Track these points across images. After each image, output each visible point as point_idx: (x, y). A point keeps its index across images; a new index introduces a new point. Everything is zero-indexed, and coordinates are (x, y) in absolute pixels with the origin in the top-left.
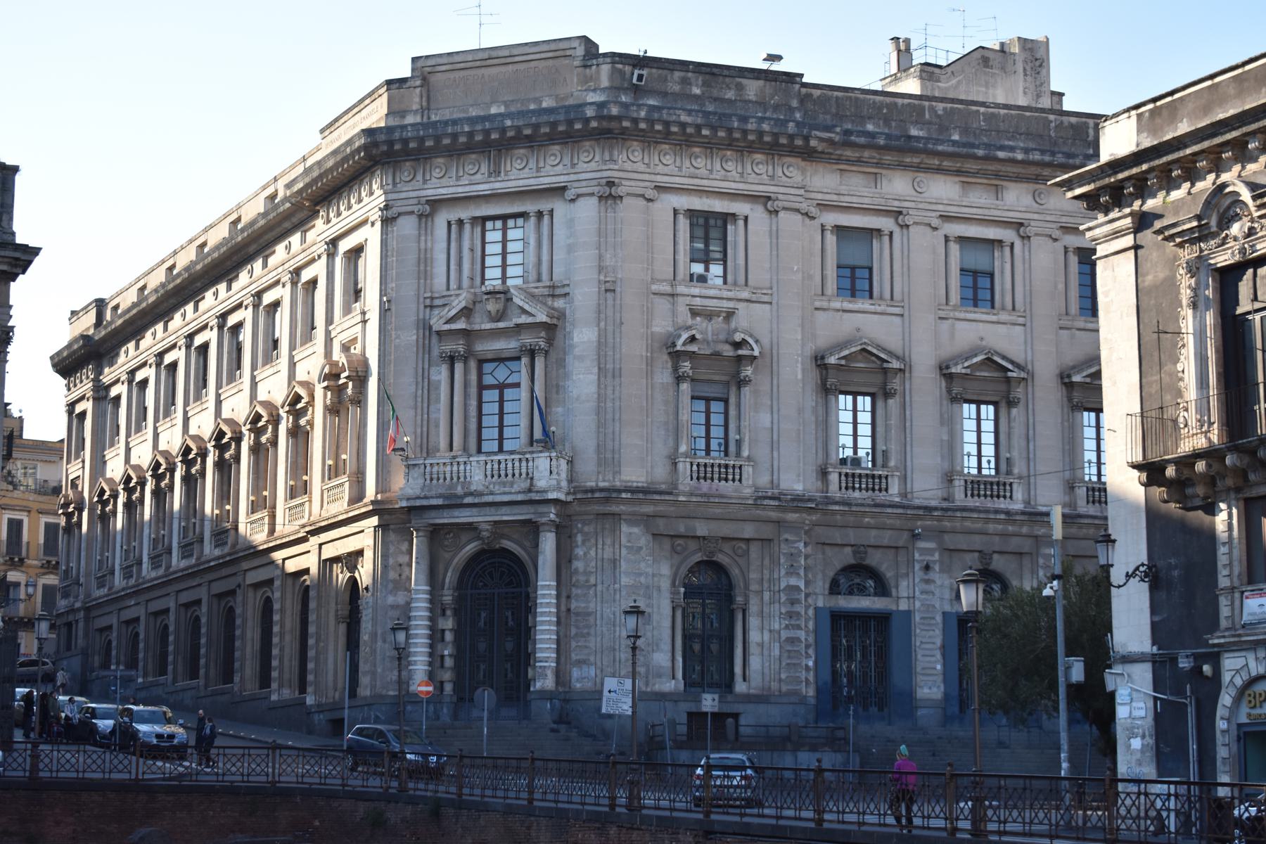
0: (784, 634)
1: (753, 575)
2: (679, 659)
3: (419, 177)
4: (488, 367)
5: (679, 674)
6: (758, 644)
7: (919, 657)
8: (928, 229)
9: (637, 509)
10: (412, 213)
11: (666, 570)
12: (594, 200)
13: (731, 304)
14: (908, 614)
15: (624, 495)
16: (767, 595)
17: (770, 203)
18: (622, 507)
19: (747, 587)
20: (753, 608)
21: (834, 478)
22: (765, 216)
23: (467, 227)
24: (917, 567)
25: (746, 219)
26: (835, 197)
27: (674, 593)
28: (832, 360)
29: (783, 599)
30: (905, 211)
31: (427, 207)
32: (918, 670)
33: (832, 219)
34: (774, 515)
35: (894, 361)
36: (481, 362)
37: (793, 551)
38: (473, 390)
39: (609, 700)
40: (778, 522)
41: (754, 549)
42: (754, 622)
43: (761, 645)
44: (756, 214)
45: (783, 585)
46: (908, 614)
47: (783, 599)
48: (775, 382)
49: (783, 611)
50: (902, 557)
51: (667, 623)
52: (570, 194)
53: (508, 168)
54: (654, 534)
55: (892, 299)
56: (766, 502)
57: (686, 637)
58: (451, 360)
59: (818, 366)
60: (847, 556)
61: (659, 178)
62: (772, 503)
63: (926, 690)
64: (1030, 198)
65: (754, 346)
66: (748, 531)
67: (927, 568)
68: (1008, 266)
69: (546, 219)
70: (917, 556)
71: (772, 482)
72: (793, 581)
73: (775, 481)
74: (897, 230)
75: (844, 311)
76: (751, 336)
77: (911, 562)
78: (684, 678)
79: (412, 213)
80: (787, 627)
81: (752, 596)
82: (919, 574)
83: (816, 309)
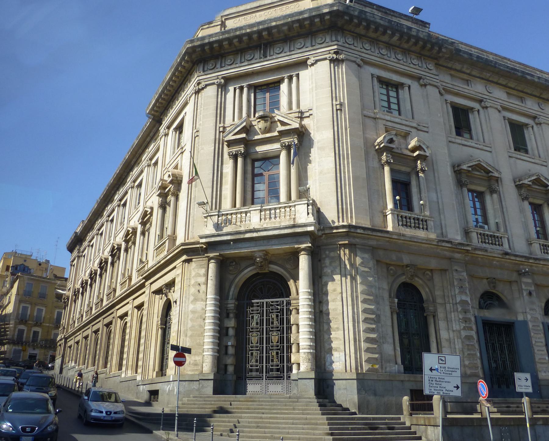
0: (464, 333)
1: (438, 293)
2: (398, 349)
3: (218, 66)
4: (257, 164)
5: (399, 360)
6: (447, 340)
7: (536, 351)
8: (497, 112)
9: (366, 242)
10: (213, 84)
11: (385, 286)
12: (328, 62)
13: (408, 129)
14: (525, 323)
15: (359, 231)
16: (448, 306)
17: (421, 80)
18: (357, 240)
19: (434, 301)
20: (441, 314)
21: (474, 235)
22: (419, 87)
23: (245, 90)
24: (525, 294)
25: (409, 87)
26: (451, 86)
27: (392, 302)
28: (465, 167)
29: (460, 309)
30: (485, 100)
31: (223, 81)
32: (537, 360)
33: (451, 98)
34: (447, 254)
35: (496, 173)
36: (254, 161)
37: (461, 277)
38: (249, 176)
39: (431, 379)
40: (450, 259)
41: (437, 278)
42: (442, 324)
43: (449, 341)
44: (415, 86)
45: (458, 300)
46: (525, 323)
47: (460, 309)
48: (436, 175)
49: (461, 317)
50: (515, 287)
51: (389, 323)
52: (309, 62)
53: (272, 53)
54: (378, 261)
55: (484, 142)
56: (444, 244)
57: (401, 334)
58: (235, 157)
59: (455, 172)
60: (484, 286)
61: (363, 55)
62: (447, 245)
63: (544, 374)
64: (537, 106)
65: (426, 150)
66: (433, 264)
67: (530, 294)
68: (533, 137)
69: (295, 79)
70: (523, 287)
71: (442, 234)
72: (464, 298)
73: (444, 233)
74: (481, 109)
75: (462, 145)
76: (424, 144)
77: (520, 291)
78: (403, 363)
79: (213, 84)
80: (464, 328)
81: (438, 306)
82: (526, 298)
83: (450, 142)
